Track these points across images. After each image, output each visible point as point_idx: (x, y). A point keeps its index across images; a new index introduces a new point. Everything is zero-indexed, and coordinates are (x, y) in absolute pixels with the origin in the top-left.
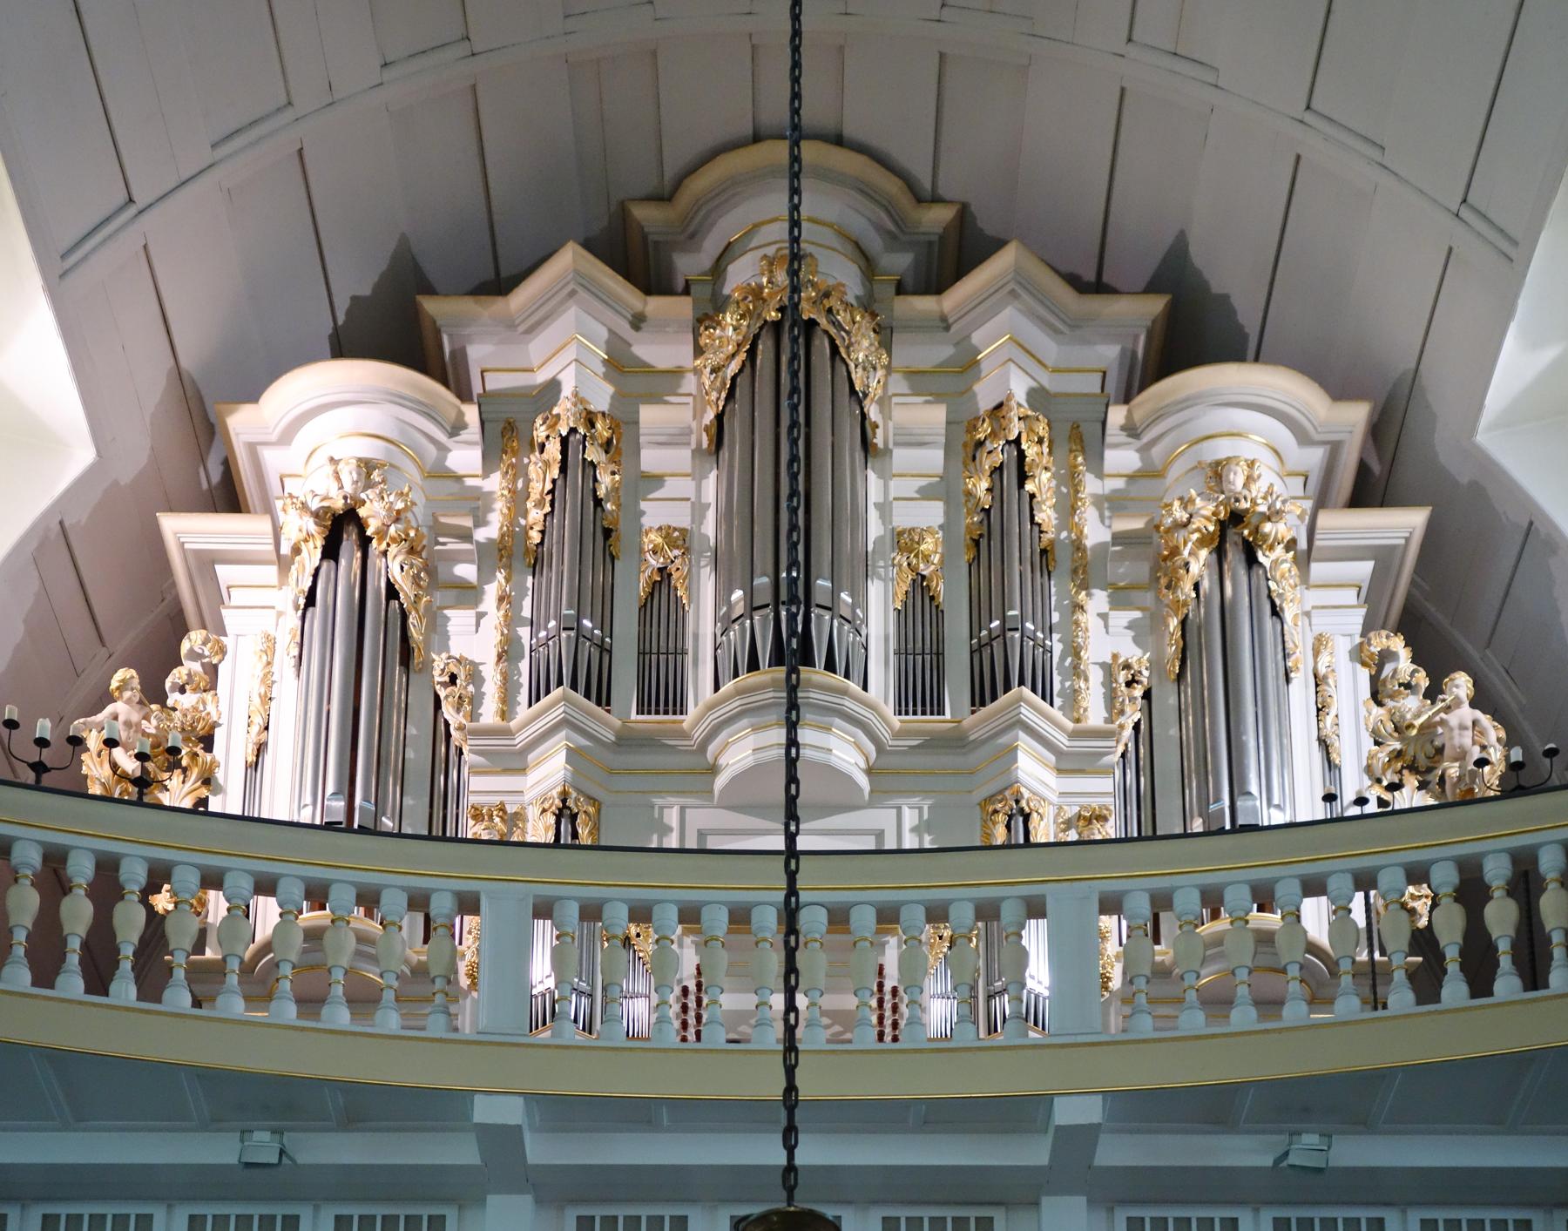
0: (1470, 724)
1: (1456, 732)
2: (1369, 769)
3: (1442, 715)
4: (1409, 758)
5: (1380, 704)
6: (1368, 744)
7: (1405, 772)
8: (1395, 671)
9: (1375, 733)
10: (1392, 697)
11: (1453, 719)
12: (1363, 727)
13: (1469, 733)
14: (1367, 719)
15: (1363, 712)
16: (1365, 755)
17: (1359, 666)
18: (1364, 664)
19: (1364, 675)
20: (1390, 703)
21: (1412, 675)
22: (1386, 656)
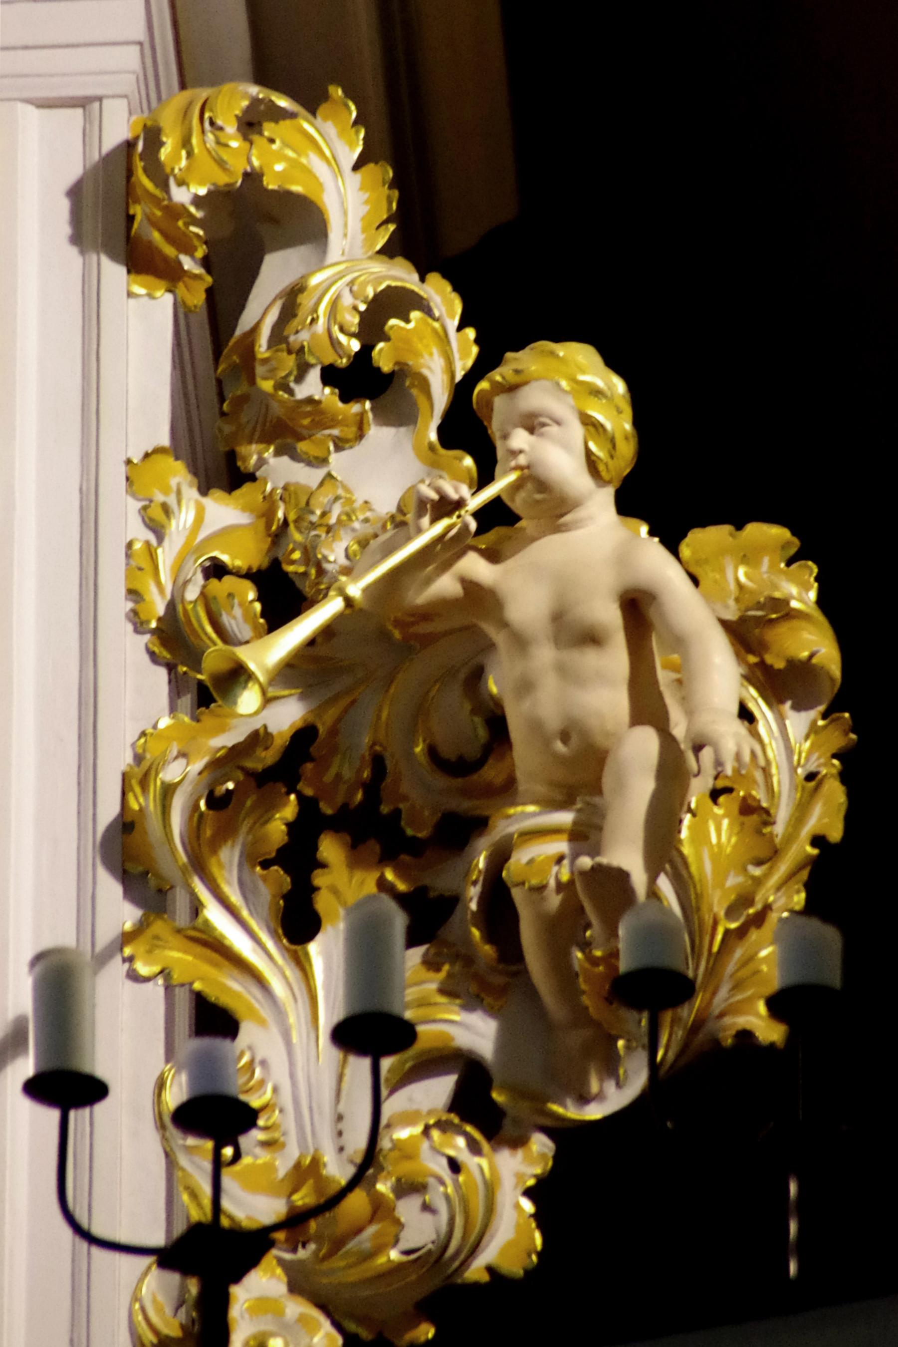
0: (609, 615)
1: (544, 655)
2: (125, 849)
3: (474, 565)
4: (345, 772)
5: (224, 473)
6: (139, 693)
7: (330, 849)
8: (291, 300)
9: (173, 641)
10: (287, 431)
11: (524, 585)
12: (114, 605)
13: (616, 659)
14: (141, 562)
15: (123, 522)
16: (115, 760)
17: (114, 273)
18: (140, 260)
19: (145, 323)
20: (279, 470)
21: (372, 326)
22: (257, 222)
